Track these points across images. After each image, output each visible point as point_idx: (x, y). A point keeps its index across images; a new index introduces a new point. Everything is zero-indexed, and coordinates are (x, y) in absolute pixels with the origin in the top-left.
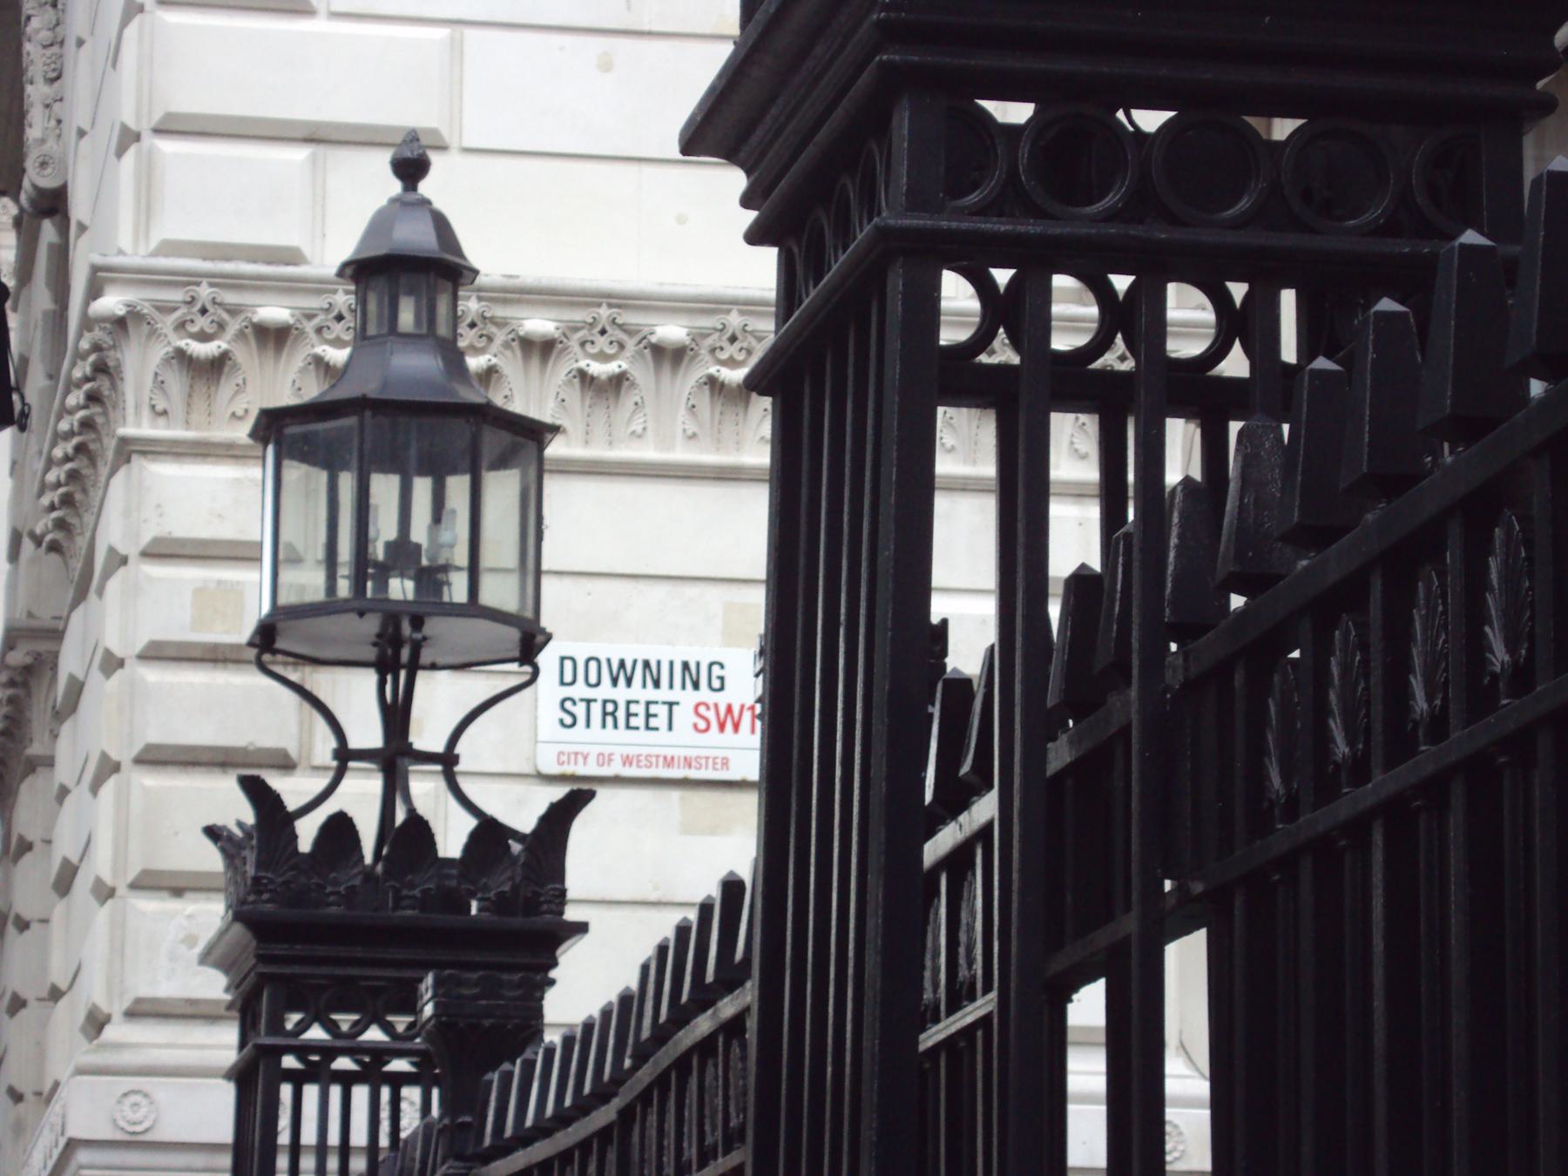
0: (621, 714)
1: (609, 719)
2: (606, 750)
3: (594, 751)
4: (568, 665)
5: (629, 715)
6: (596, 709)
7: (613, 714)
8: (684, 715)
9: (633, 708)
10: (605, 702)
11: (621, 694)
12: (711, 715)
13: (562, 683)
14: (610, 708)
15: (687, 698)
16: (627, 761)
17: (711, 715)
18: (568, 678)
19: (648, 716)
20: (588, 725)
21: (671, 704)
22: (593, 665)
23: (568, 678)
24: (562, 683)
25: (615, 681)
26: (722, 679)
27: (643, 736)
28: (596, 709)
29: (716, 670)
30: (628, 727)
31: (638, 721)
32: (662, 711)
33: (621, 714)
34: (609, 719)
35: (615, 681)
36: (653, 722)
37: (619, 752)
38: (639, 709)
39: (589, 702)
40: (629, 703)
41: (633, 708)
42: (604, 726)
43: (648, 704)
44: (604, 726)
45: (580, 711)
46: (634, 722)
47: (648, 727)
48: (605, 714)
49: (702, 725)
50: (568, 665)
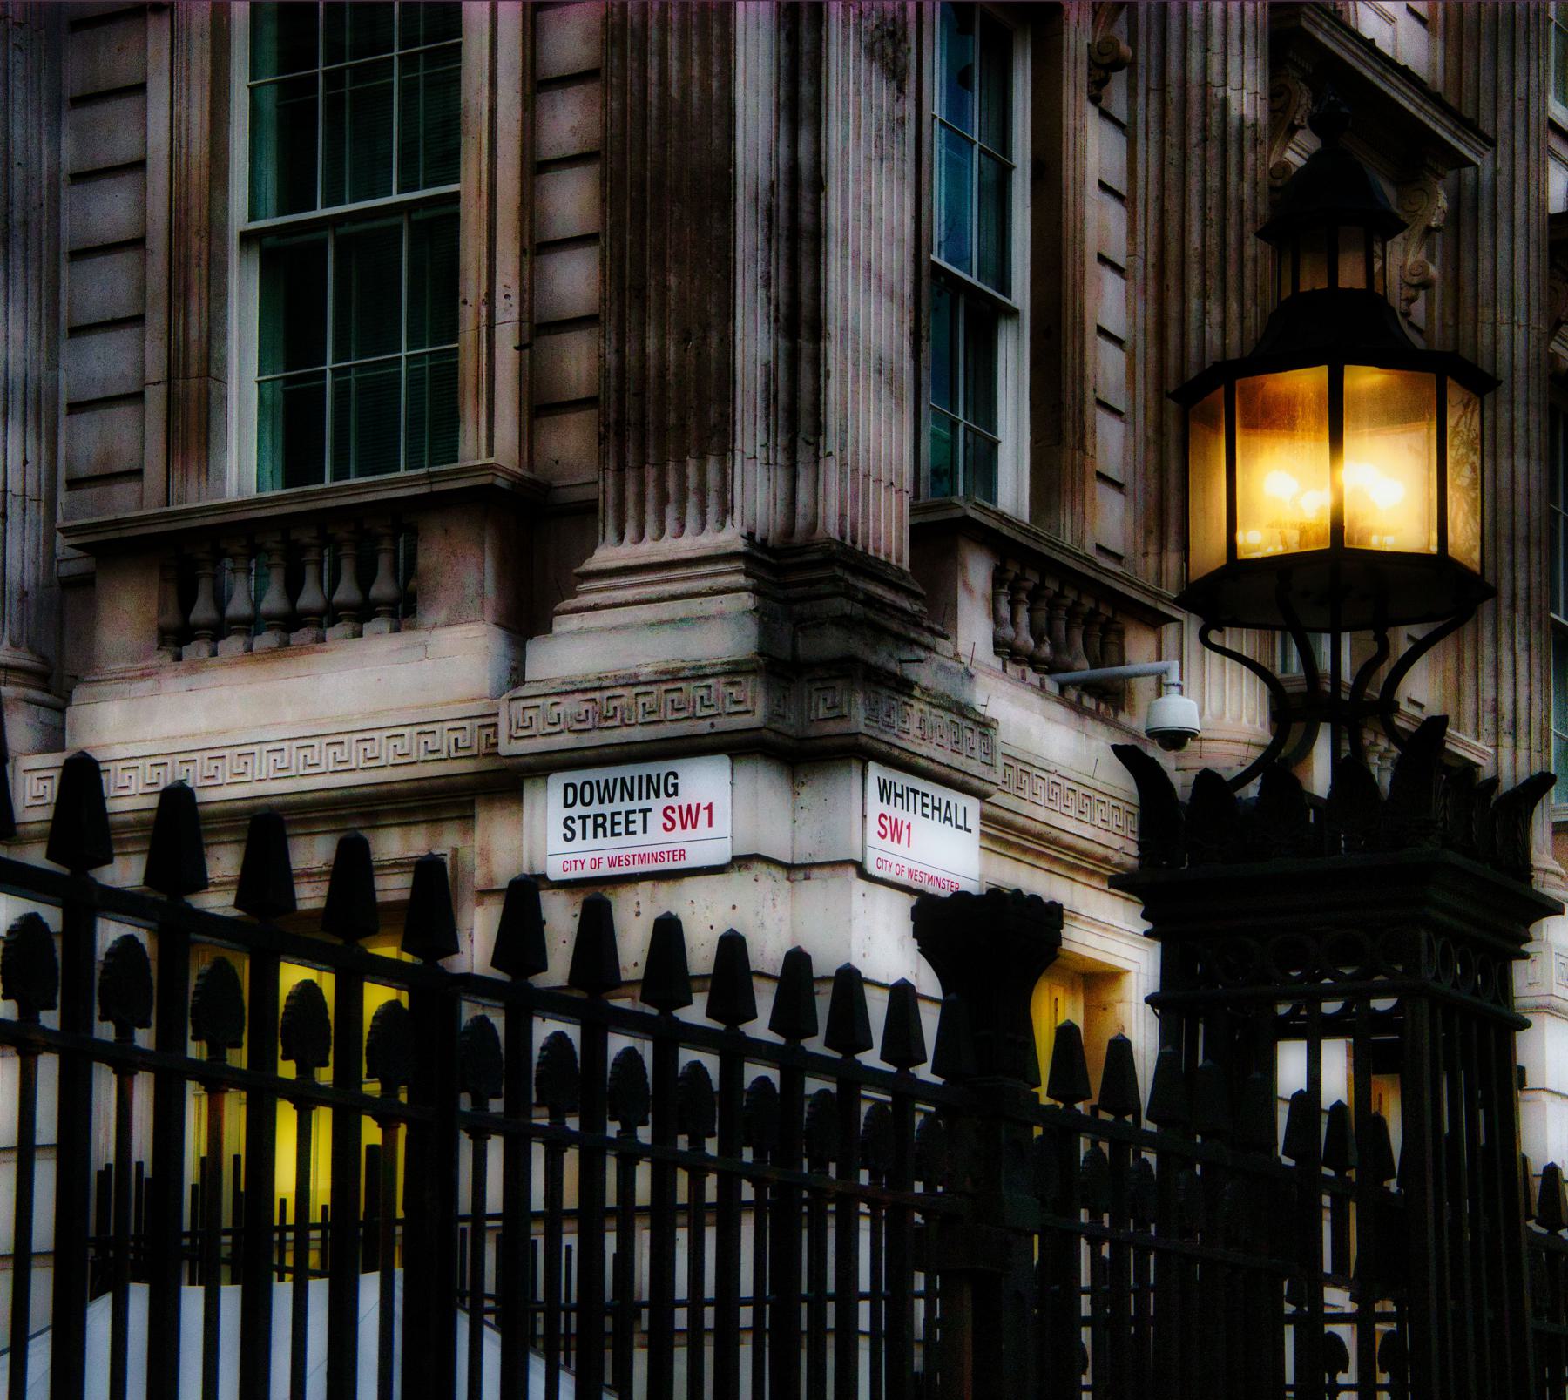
0: (608, 825)
1: (600, 830)
2: (597, 855)
3: (587, 857)
4: (570, 790)
5: (614, 824)
6: (590, 822)
7: (603, 826)
8: (656, 819)
9: (617, 819)
10: (596, 816)
11: (607, 809)
12: (676, 816)
13: (566, 805)
14: (600, 820)
15: (657, 804)
16: (612, 862)
17: (676, 816)
18: (570, 801)
19: (628, 822)
20: (584, 837)
21: (645, 812)
22: (587, 788)
23: (570, 801)
24: (566, 805)
25: (602, 802)
26: (675, 786)
27: (624, 840)
28: (590, 822)
29: (671, 779)
30: (613, 834)
31: (620, 829)
32: (638, 817)
33: (608, 825)
34: (600, 830)
35: (602, 802)
36: (632, 827)
37: (605, 855)
38: (621, 818)
39: (584, 818)
40: (613, 815)
41: (617, 819)
42: (595, 836)
43: (628, 813)
44: (595, 836)
45: (578, 826)
46: (617, 829)
47: (628, 833)
48: (596, 826)
49: (669, 825)
50: (570, 790)
